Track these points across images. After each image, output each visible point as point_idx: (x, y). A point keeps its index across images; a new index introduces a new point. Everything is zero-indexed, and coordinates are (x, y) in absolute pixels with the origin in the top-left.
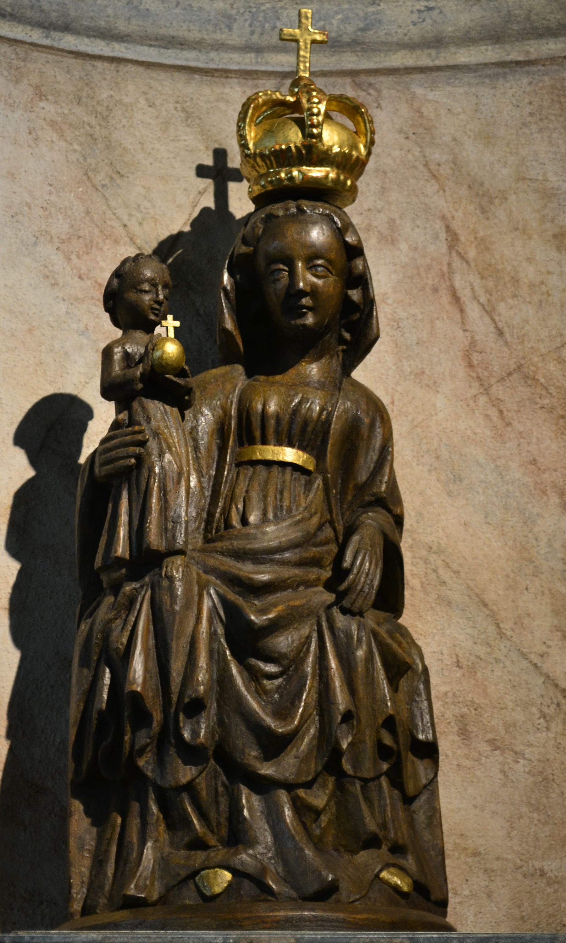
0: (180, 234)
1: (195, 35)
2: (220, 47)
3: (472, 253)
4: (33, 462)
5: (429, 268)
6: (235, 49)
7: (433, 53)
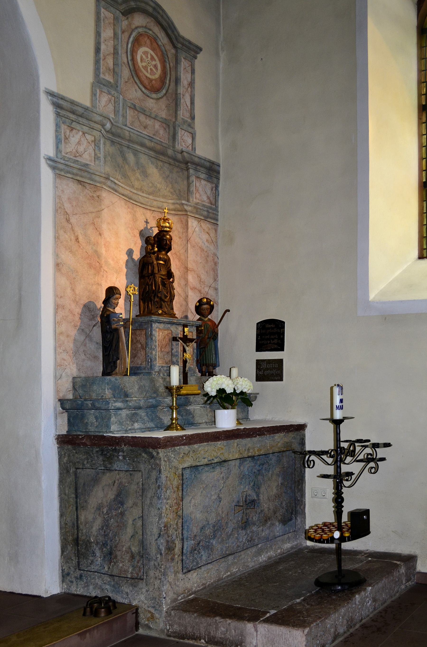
1: (144, 203)
2: (147, 205)
4: (128, 257)
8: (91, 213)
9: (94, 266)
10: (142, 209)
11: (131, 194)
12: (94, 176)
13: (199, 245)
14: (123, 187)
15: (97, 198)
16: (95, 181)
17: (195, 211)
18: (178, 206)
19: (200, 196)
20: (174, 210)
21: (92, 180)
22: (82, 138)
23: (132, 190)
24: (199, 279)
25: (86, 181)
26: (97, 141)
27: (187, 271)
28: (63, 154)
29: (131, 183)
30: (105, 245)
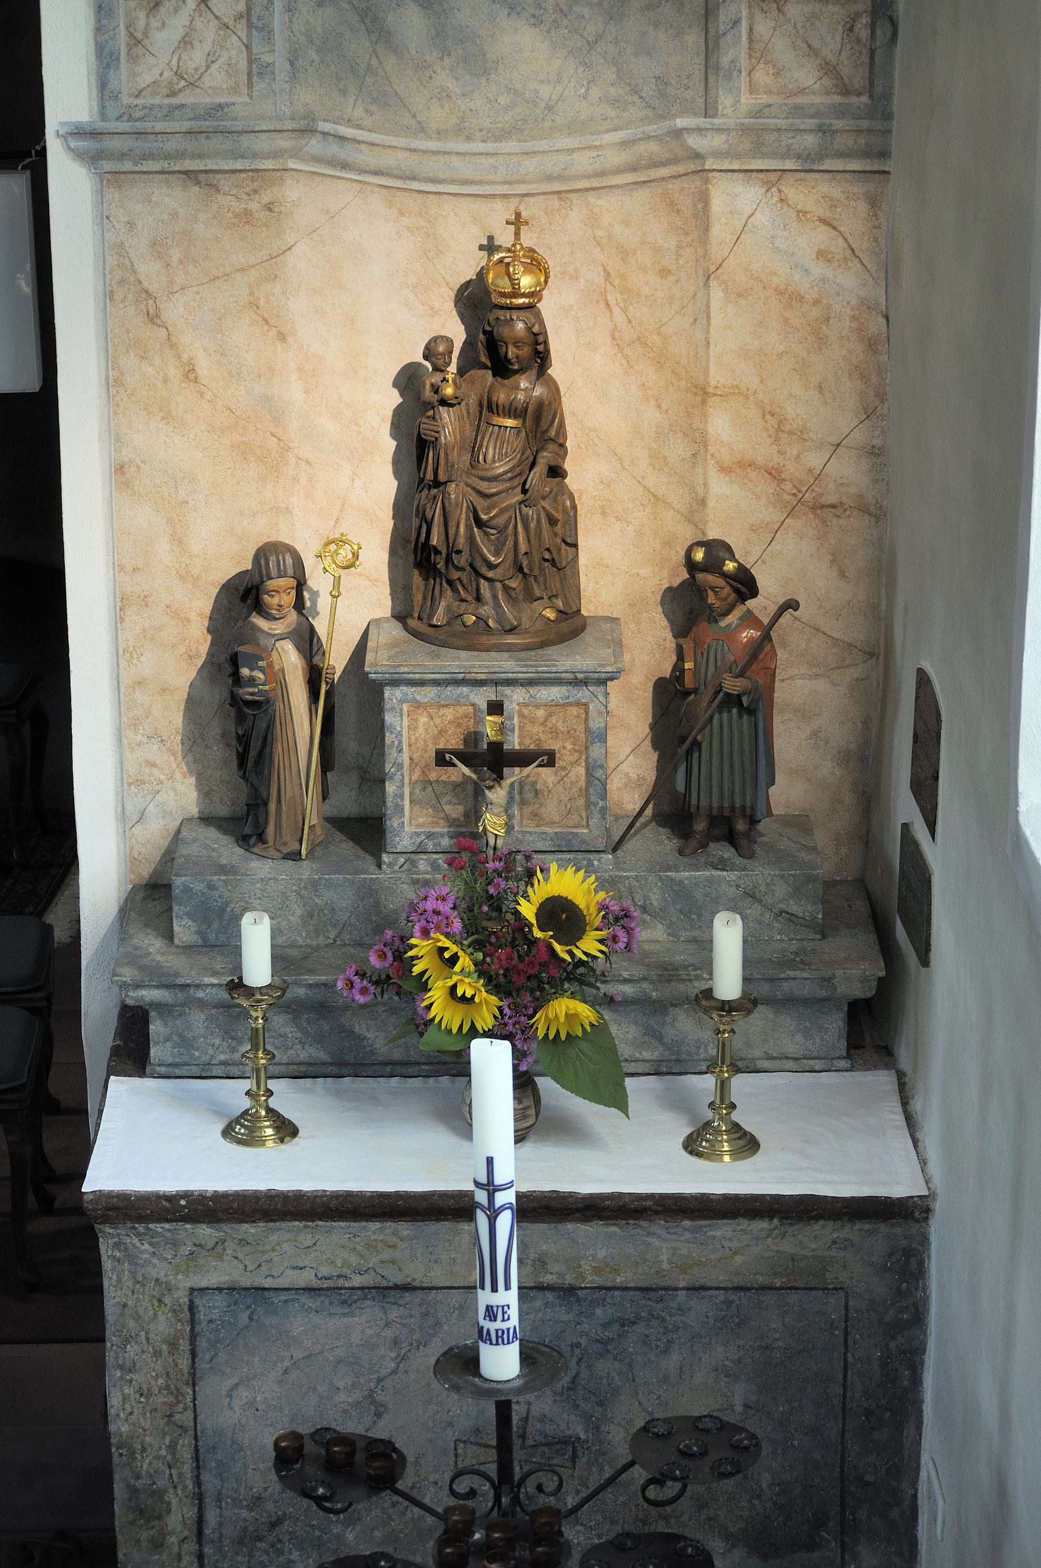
0: (471, 280)
1: (477, 178)
2: (492, 183)
3: (617, 282)
4: (401, 395)
5: (595, 290)
6: (498, 183)
7: (600, 179)
8: (242, 270)
9: (258, 451)
10: (465, 204)
11: (415, 157)
12: (246, 141)
13: (775, 280)
14: (377, 141)
15: (264, 214)
16: (255, 156)
17: (747, 145)
18: (653, 147)
19: (777, 74)
20: (633, 168)
21: (242, 157)
22: (197, 19)
23: (415, 144)
24: (774, 422)
25: (215, 167)
26: (257, 10)
27: (704, 402)
28: (126, 100)
29: (414, 116)
30: (300, 370)
